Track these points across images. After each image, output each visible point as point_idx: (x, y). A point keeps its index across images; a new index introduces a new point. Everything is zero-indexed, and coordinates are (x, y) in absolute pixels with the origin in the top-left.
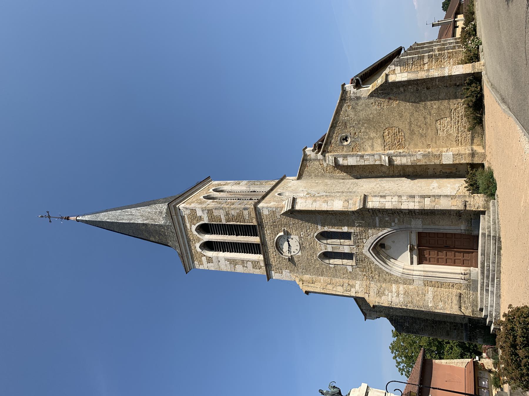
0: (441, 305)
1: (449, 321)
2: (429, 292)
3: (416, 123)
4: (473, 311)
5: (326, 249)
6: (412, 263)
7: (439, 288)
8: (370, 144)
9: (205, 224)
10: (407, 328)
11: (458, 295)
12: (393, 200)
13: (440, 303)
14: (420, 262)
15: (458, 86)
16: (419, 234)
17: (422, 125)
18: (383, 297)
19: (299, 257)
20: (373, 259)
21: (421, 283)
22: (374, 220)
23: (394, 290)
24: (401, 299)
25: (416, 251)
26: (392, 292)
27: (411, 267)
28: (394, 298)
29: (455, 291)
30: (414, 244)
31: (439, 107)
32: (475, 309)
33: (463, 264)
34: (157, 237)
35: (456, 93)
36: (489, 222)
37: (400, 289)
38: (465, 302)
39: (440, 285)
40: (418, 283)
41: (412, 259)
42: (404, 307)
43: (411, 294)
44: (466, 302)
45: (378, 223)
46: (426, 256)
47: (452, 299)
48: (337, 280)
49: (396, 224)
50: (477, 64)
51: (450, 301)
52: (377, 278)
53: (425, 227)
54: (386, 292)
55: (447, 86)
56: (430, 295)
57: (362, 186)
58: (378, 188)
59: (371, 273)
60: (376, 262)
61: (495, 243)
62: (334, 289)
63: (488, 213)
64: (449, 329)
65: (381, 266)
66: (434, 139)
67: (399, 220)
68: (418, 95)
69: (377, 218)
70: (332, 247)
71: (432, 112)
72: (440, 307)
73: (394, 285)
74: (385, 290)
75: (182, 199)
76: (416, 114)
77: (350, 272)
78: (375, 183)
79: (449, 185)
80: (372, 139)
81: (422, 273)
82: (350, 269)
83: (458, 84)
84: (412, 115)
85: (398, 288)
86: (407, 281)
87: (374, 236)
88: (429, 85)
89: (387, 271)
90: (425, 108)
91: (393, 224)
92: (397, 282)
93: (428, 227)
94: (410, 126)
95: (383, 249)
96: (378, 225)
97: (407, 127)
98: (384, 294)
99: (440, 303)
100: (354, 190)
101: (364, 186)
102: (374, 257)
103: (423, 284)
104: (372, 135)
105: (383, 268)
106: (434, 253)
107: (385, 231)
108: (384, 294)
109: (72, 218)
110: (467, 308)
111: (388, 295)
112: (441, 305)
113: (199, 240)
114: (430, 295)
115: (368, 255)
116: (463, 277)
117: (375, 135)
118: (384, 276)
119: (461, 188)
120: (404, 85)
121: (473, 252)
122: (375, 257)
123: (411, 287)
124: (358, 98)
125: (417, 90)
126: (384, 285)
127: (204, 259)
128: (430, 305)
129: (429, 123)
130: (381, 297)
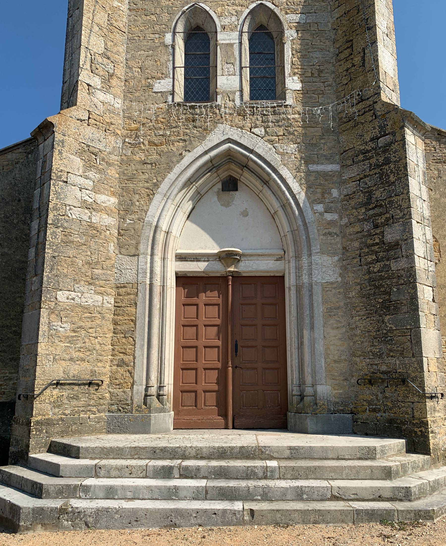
0: (64, 328)
2: (99, 298)
4: (49, 423)
5: (224, 27)
7: (111, 327)
11: (95, 380)
13: (67, 326)
14: (182, 279)
16: (277, 282)
18: (78, 162)
20: (200, 150)
21: (129, 276)
22: (329, 159)
23: (101, 198)
24: (75, 213)
25: (218, 268)
26: (95, 190)
27: (171, 256)
28: (79, 194)
29: (105, 369)
32: (57, 429)
33: (181, 390)
37: (105, 216)
38: (76, 398)
39: (125, 327)
40: (128, 269)
41: (196, 258)
42: (51, 216)
43: (92, 244)
44: (74, 402)
45: (320, 168)
46: (203, 296)
47: (83, 360)
48: (122, 49)
51: (75, 355)
52: (137, 158)
53: (317, 290)
56: (91, 298)
59: (151, 143)
60: (193, 159)
61: (380, 498)
62: (96, 28)
65: (177, 170)
67: (331, 223)
69: (336, 167)
72: (57, 323)
73: (114, 200)
74: (100, 171)
77: (150, 87)
81: (157, 282)
82: (162, 85)
85: (107, 211)
86: (132, 237)
87: (278, 157)
89: (164, 187)
91: (320, 208)
92: (125, 209)
95: (219, 186)
96: (313, 167)
99: (67, 326)
102: (206, 152)
103: (122, 280)
105: (172, 176)
106: (213, 314)
107: (295, 186)
108: (89, 166)
110: (57, 404)
111: (87, 178)
112: (64, 328)
114: (91, 298)
115: (214, 138)
116: (153, 391)
121: (225, 416)
122: (206, 158)
123: (112, 247)
126: (113, 172)
128: (62, 296)
130: (80, 153)
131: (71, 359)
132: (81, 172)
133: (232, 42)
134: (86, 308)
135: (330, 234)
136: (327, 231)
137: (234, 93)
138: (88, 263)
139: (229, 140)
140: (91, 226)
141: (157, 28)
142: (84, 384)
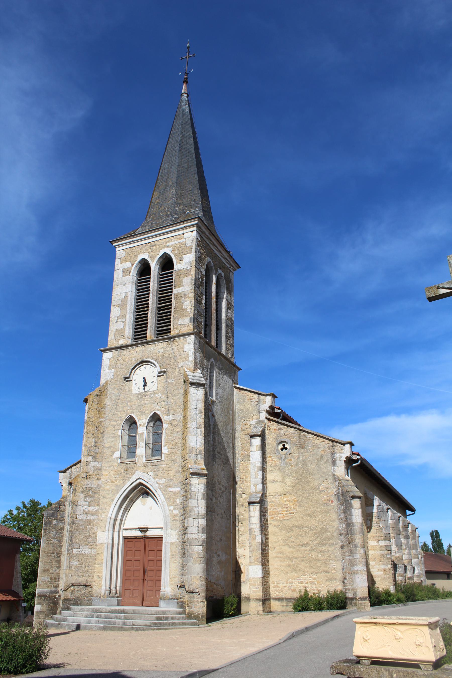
1: (61, 572)
2: (90, 550)
3: (301, 533)
6: (126, 529)
8: (277, 478)
9: (173, 266)
10: (50, 523)
12: (200, 508)
15: (344, 582)
17: (298, 540)
18: (82, 495)
19: (130, 390)
22: (177, 485)
23: (91, 508)
24: (79, 517)
26: (89, 505)
30: (148, 532)
31: (319, 560)
34: (157, 201)
35: (335, 579)
36: (172, 618)
44: (79, 592)
47: (83, 576)
49: (172, 511)
50: (367, 602)
51: (80, 574)
53: (168, 546)
54: (89, 499)
55: (343, 569)
57: (223, 470)
58: (220, 489)
63: (183, 617)
64: (51, 571)
66: (281, 555)
67: (176, 515)
68: (335, 534)
70: (143, 433)
71: (314, 553)
74: (92, 497)
75: (207, 233)
76: (311, 533)
78: (226, 485)
79: (223, 573)
80: (283, 481)
83: (345, 581)
84: (311, 528)
87: (157, 485)
88: (346, 549)
90: (318, 544)
91: (171, 508)
93: (168, 550)
94: (298, 527)
97: (296, 523)
98: (87, 495)
100: (217, 460)
101: (223, 472)
102: (131, 484)
104: (288, 481)
108: (87, 495)
109: (184, 87)
111: (86, 501)
113: (152, 257)
117: (288, 484)
118: (109, 496)
119: (219, 587)
120: (346, 518)
124: (334, 463)
125: (341, 534)
127: (128, 264)
129: (301, 549)
131: (78, 576)
132: (83, 499)
133: (143, 432)
134: (84, 555)
135: (175, 520)
136: (174, 519)
137: (142, 456)
138: (86, 536)
139: (139, 478)
140: (88, 521)
141: (116, 427)
142: (83, 585)
